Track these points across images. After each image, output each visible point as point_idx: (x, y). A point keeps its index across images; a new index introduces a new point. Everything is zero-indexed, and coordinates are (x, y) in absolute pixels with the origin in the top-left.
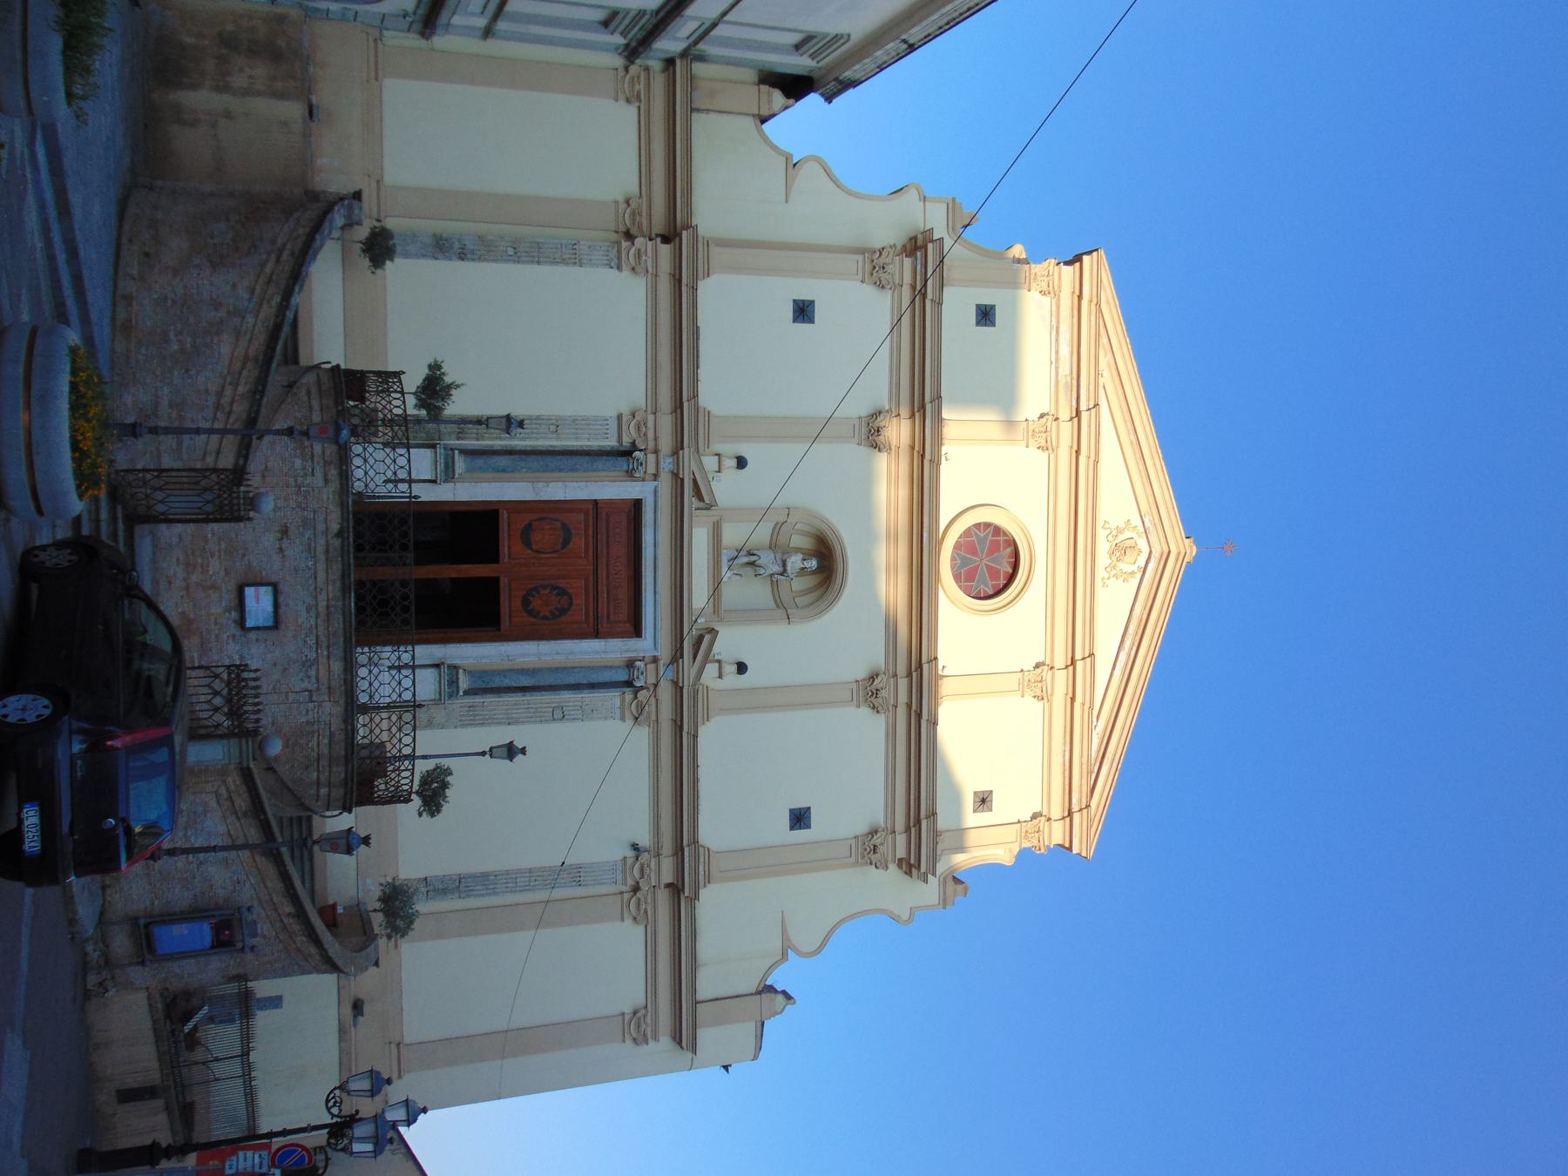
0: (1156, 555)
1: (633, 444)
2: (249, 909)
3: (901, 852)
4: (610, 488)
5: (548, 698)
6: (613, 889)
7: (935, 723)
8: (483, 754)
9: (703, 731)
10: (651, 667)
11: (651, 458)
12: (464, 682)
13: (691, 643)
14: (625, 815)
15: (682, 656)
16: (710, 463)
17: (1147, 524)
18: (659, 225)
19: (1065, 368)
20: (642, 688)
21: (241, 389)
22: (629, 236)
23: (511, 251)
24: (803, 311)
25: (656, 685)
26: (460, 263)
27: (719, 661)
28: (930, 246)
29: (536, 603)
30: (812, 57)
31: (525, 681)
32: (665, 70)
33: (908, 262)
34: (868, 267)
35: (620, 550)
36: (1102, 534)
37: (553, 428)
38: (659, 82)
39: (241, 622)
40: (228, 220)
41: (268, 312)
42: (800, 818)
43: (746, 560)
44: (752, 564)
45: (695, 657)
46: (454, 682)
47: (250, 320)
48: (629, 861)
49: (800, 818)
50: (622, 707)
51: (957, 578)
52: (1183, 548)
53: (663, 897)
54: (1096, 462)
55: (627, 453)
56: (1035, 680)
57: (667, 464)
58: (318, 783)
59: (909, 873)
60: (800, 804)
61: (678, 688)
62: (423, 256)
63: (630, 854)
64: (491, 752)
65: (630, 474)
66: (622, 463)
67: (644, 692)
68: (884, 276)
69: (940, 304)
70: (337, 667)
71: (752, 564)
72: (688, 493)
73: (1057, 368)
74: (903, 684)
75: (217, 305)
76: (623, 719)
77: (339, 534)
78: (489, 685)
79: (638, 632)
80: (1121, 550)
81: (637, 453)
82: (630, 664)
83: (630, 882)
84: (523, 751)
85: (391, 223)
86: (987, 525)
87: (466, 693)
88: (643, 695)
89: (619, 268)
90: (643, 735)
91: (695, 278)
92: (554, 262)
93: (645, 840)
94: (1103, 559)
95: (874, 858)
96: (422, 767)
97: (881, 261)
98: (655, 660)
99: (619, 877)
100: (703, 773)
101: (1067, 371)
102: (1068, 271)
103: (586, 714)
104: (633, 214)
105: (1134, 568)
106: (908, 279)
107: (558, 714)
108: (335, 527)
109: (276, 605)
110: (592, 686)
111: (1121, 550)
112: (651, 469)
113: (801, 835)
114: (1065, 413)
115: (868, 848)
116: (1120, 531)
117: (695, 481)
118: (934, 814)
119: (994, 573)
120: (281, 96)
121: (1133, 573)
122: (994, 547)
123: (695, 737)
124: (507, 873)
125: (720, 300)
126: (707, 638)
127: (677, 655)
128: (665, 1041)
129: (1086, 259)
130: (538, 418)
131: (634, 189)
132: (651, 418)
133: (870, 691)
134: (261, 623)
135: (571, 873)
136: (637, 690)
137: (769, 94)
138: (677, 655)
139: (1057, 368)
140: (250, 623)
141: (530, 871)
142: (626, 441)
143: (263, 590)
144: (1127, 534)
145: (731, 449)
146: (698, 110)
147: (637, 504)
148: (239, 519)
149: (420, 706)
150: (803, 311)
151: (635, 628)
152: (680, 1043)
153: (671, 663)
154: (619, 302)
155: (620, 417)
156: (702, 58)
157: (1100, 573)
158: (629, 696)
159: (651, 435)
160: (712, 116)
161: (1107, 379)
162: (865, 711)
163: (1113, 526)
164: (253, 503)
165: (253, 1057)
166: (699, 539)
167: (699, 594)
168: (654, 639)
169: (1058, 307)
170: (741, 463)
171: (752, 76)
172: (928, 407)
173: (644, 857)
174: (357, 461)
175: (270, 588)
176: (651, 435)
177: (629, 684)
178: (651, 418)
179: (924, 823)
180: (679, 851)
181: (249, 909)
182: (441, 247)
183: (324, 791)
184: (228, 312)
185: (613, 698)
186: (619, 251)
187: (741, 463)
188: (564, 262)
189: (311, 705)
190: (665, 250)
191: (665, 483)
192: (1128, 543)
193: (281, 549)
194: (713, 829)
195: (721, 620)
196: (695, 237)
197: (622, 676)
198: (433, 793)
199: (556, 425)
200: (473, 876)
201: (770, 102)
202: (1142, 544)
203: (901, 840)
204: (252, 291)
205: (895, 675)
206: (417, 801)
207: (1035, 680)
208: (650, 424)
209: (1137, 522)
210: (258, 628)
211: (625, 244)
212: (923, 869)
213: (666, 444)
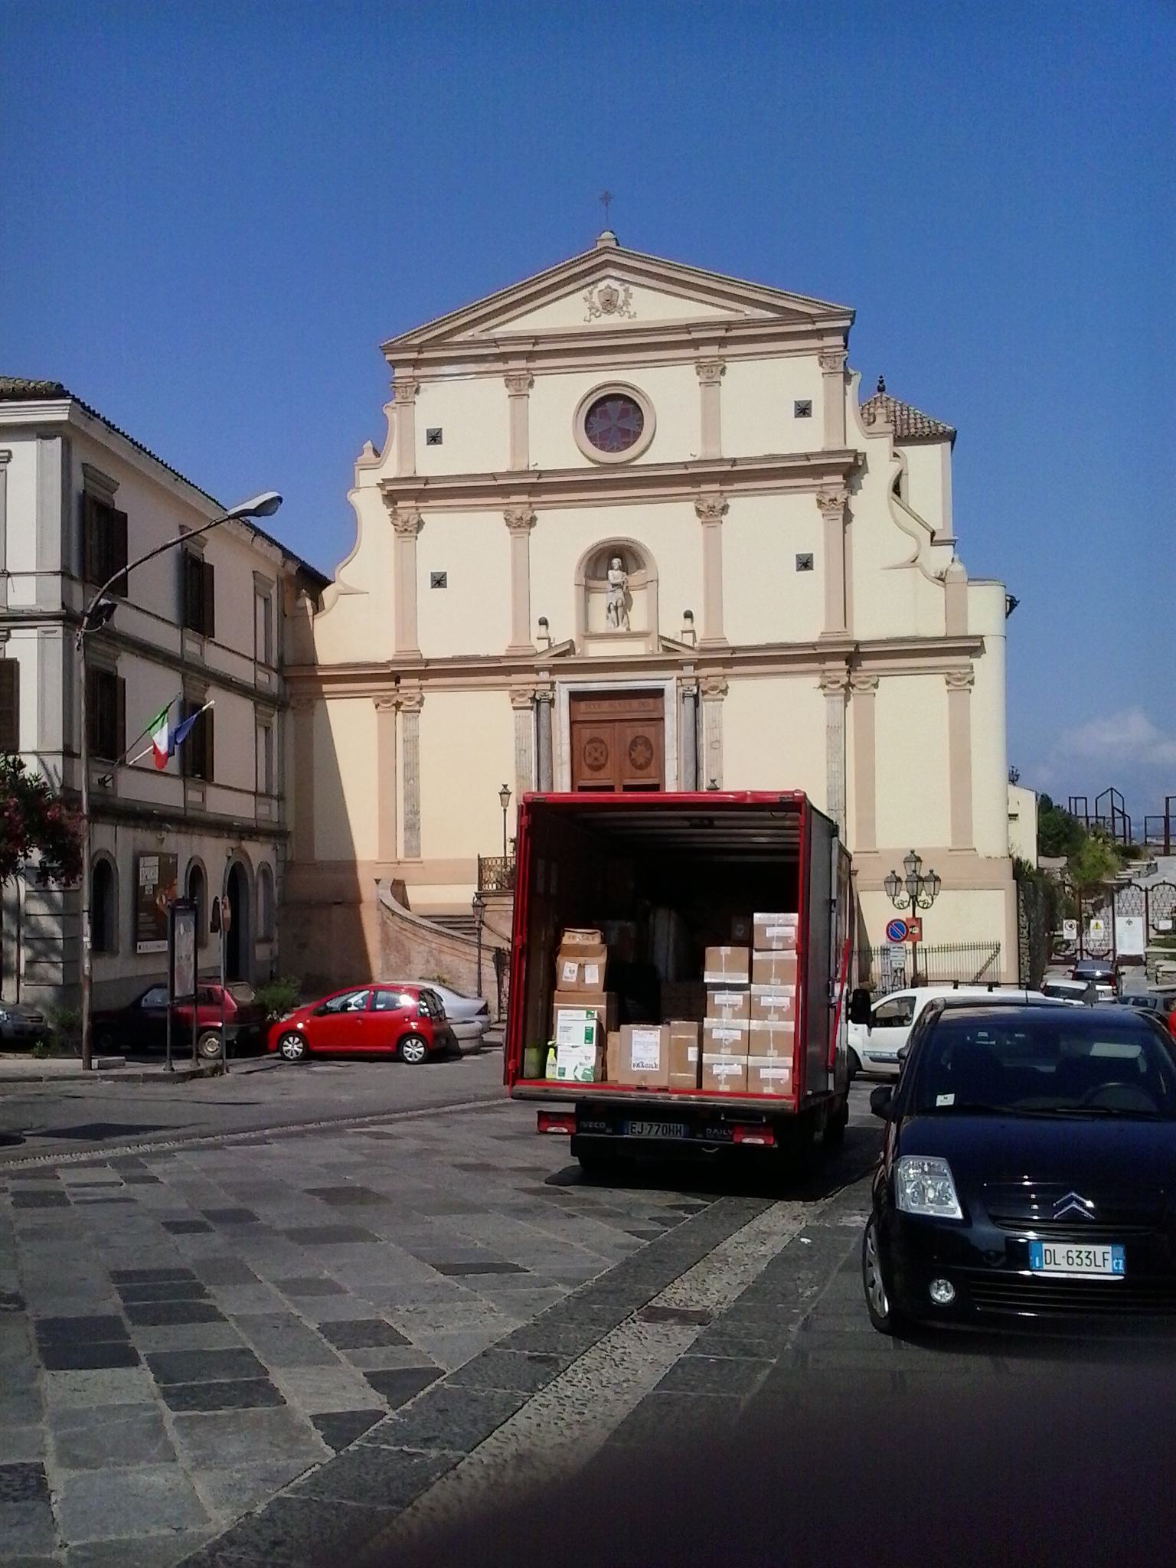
4: (561, 715)
9: (733, 643)
14: (802, 694)
16: (542, 646)
22: (398, 705)
29: (641, 761)
30: (271, 587)
41: (429, 936)
42: (805, 563)
44: (616, 608)
50: (714, 700)
51: (627, 445)
56: (711, 373)
57: (544, 676)
61: (698, 664)
62: (418, 837)
65: (552, 702)
66: (544, 706)
72: (565, 661)
75: (428, 961)
79: (659, 693)
80: (609, 304)
84: (713, 781)
92: (417, 753)
93: (816, 680)
100: (762, 642)
103: (716, 725)
105: (621, 289)
107: (716, 745)
119: (624, 414)
122: (605, 414)
127: (676, 665)
128: (974, 661)
132: (514, 687)
133: (712, 514)
142: (529, 704)
150: (439, 581)
166: (598, 651)
167: (636, 649)
177: (696, 697)
178: (514, 687)
180: (823, 658)
185: (705, 707)
188: (416, 746)
191: (557, 678)
197: (690, 702)
199: (521, 751)
202: (602, 285)
207: (711, 373)
211: (402, 708)
213: (533, 677)
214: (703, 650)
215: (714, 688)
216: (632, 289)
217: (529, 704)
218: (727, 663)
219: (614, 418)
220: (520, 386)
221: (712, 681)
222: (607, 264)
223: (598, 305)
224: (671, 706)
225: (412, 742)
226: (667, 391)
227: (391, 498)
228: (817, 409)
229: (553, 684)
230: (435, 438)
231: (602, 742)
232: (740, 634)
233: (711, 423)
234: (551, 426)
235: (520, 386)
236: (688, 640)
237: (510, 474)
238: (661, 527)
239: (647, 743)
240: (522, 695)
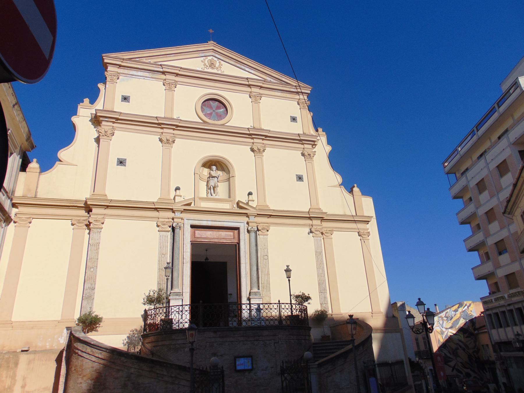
0: (213, 54)
1: (170, 227)
2: (364, 363)
3: (310, 146)
5: (259, 261)
6: (322, 240)
8: (289, 280)
12: (255, 290)
13: (241, 209)
15: (247, 214)
17: (203, 55)
18: (83, 212)
19: (147, 74)
20: (257, 228)
21: (165, 373)
23: (92, 270)
24: (121, 162)
26: (96, 289)
27: (248, 201)
28: (98, 114)
31: (255, 268)
32: (17, 207)
33: (104, 123)
34: (105, 137)
36: (206, 70)
37: (163, 256)
38: (21, 209)
39: (250, 371)
40: (81, 383)
43: (212, 190)
44: (214, 188)
45: (247, 209)
46: (256, 293)
47: (132, 370)
48: (314, 235)
49: (300, 178)
52: (211, 45)
53: (325, 224)
54: (181, 68)
55: (173, 229)
56: (256, 98)
57: (178, 214)
58: (305, 340)
59: (316, 145)
60: (295, 178)
62: (92, 304)
63: (311, 234)
64: (289, 277)
66: (177, 231)
67: (259, 227)
68: (109, 132)
69: (121, 113)
70: (266, 333)
71: (214, 188)
73: (146, 77)
74: (256, 140)
76: (267, 235)
77: (215, 332)
78: (256, 281)
79: (238, 229)
80: (212, 65)
81: (174, 225)
82: (248, 231)
84: (288, 266)
85: (77, 316)
86: (202, 107)
87: (259, 289)
89: (102, 228)
90: (272, 228)
91: (107, 200)
94: (215, 71)
95: (312, 155)
96: (293, 302)
97: (103, 132)
98: (248, 223)
99: (319, 239)
101: (148, 74)
102: (110, 68)
104: (79, 223)
105: (218, 62)
106: (111, 124)
108: (212, 334)
109: (244, 357)
110: (257, 245)
111: (212, 65)
112: (180, 220)
113: (305, 178)
114: (163, 77)
116: (205, 65)
117: (184, 205)
118: (299, 135)
120: (16, 364)
121: (219, 62)
123: (274, 210)
124: (318, 276)
125: (114, 193)
126: (241, 204)
128: (368, 226)
129: (106, 61)
131: (69, 222)
134: (250, 362)
135: (318, 254)
136: (258, 230)
137: (31, 168)
139: (146, 77)
140: (250, 367)
143: (237, 363)
144: (206, 62)
145: (172, 194)
146: (36, 195)
147: (192, 227)
148: (223, 372)
149: (279, 301)
150: (121, 162)
152: (369, 221)
153: (249, 217)
154: (114, 229)
156: (13, 192)
157: (219, 72)
159: (167, 220)
160: (39, 190)
161: (152, 61)
162: (264, 154)
163: (203, 67)
164: (215, 366)
165: (390, 362)
167: (226, 206)
168: (240, 222)
169: (123, 74)
170: (178, 189)
171: (22, 174)
172: (160, 122)
173: (313, 230)
174: (181, 326)
175: (237, 359)
176: (167, 220)
178: (160, 220)
179: (302, 138)
181: (364, 363)
182: (88, 297)
183: (307, 338)
184: (128, 380)
185: (260, 238)
186: (94, 228)
187: (178, 189)
188: (98, 249)
189: (280, 343)
190: (95, 210)
191: (184, 215)
192: (209, 62)
193: (222, 356)
194: (304, 207)
195: (234, 199)
196: (90, 199)
197: (253, 234)
198: (303, 299)
200: (319, 288)
201: (34, 168)
203: (306, 146)
204: (118, 370)
205: (253, 143)
206: (306, 304)
207: (256, 98)
208: (163, 220)
209: (202, 58)
210: (252, 364)
211: (92, 226)
212: (315, 140)
213: (170, 214)
215: (263, 229)
216: (222, 62)
220: (170, 86)
223: (207, 64)
225: (94, 247)
226: (238, 102)
227: (96, 121)
228: (299, 119)
230: (125, 99)
232: (275, 204)
233: (256, 115)
234: (186, 102)
235: (170, 86)
237: (165, 118)
238: (236, 154)
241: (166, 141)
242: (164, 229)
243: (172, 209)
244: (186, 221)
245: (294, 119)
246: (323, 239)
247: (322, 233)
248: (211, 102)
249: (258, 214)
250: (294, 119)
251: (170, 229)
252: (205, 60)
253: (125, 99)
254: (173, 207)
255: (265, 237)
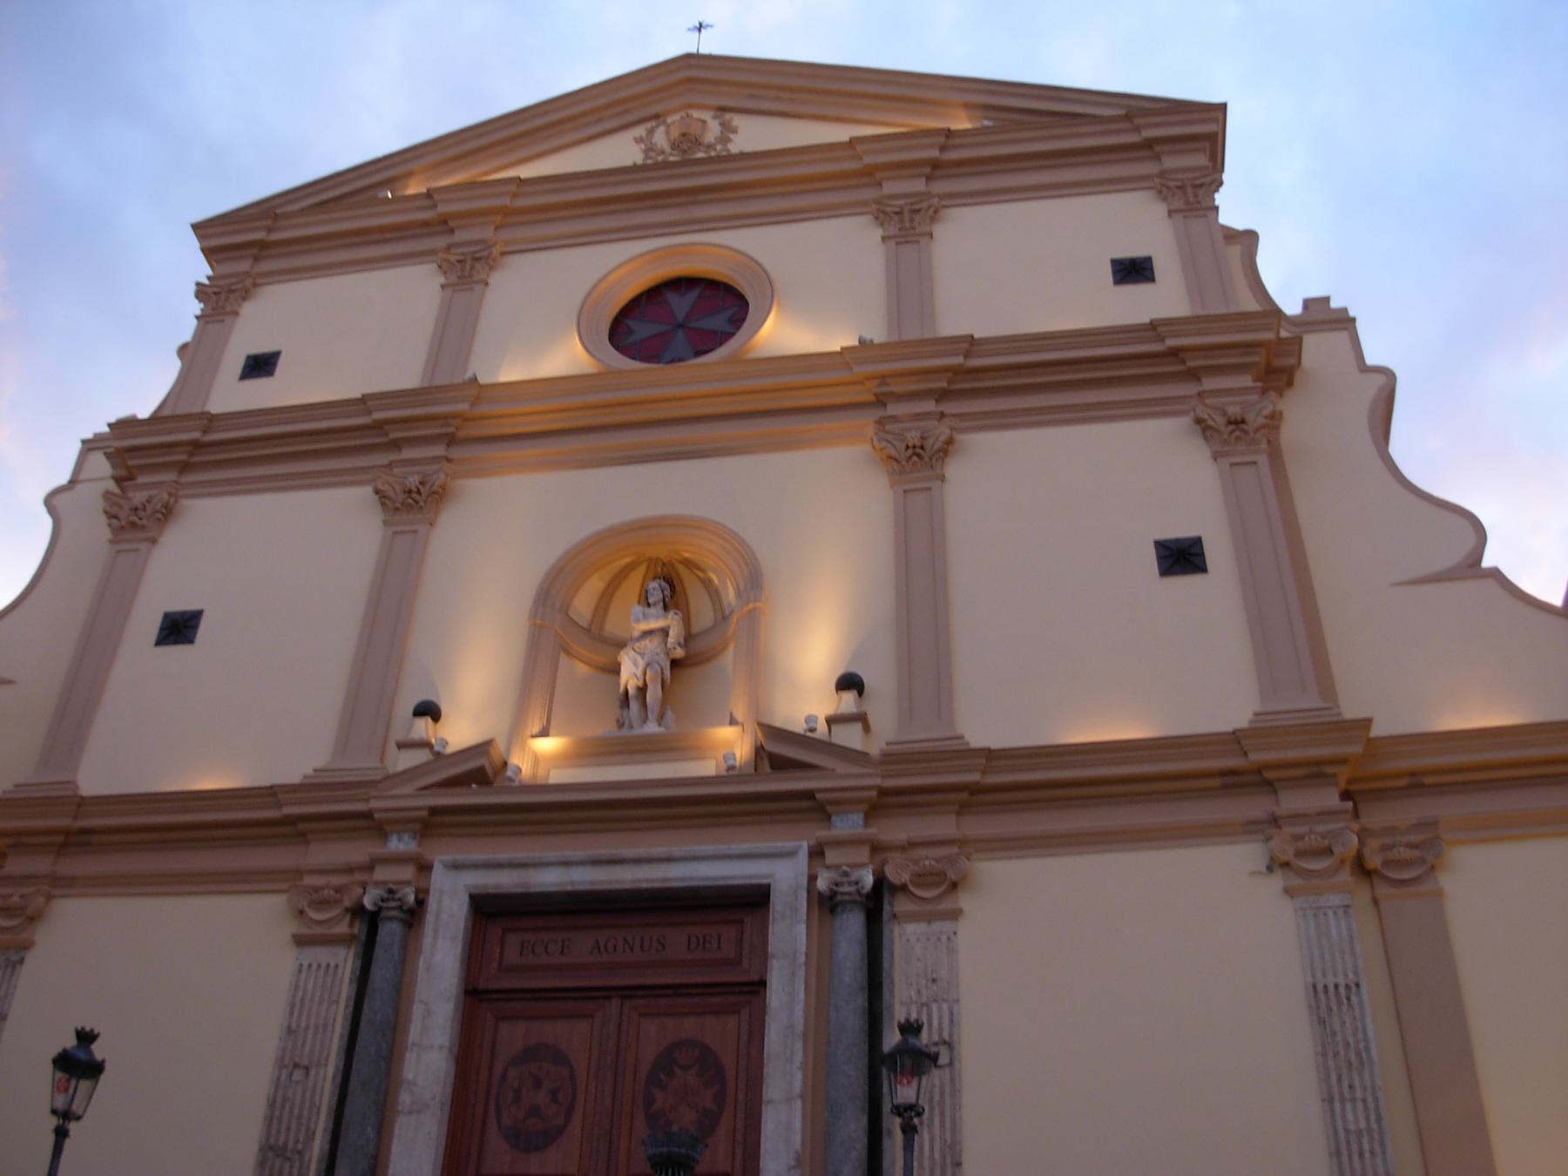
7: (970, 340)
10: (832, 857)
11: (381, 874)
15: (809, 795)
25: (876, 848)
35: (584, 945)
37: (298, 1075)
42: (1181, 557)
48: (1297, 881)
49: (1181, 557)
50: (929, 918)
53: (1378, 816)
61: (882, 803)
65: (414, 915)
66: (390, 931)
76: (955, 914)
79: (755, 899)
81: (368, 902)
82: (827, 904)
83: (1345, 876)
88: (894, 874)
98: (817, 853)
112: (407, 873)
113: (1217, 552)
115: (1243, 438)
127: (814, 807)
130: (272, 1104)
132: (309, 880)
135: (1329, 1001)
138: (814, 807)
141: (1330, 1100)
142: (343, 928)
147: (489, 911)
151: (753, 901)
155: (300, 941)
158: (902, 905)
159: (337, 880)
168: (781, 866)
176: (337, 880)
178: (309, 880)
185: (908, 940)
199: (291, 1066)
209: (640, 131)
214: (893, 759)
216: (738, 120)
217: (343, 928)
218: (973, 799)
219: (681, 318)
221: (929, 858)
222: (689, 80)
224: (789, 933)
229: (425, 868)
230: (261, 365)
231: (560, 1058)
236: (850, 737)
239: (708, 1063)
240: (322, 904)
241: (401, 497)
242: (319, 930)
243: (367, 815)
244: (440, 879)
245: (1133, 271)
246: (1375, 902)
247: (1362, 870)
248: (672, 298)
249: (883, 792)
250: (1133, 271)
251: (359, 929)
252: (651, 132)
253: (261, 365)
254: (373, 804)
255: (938, 926)
